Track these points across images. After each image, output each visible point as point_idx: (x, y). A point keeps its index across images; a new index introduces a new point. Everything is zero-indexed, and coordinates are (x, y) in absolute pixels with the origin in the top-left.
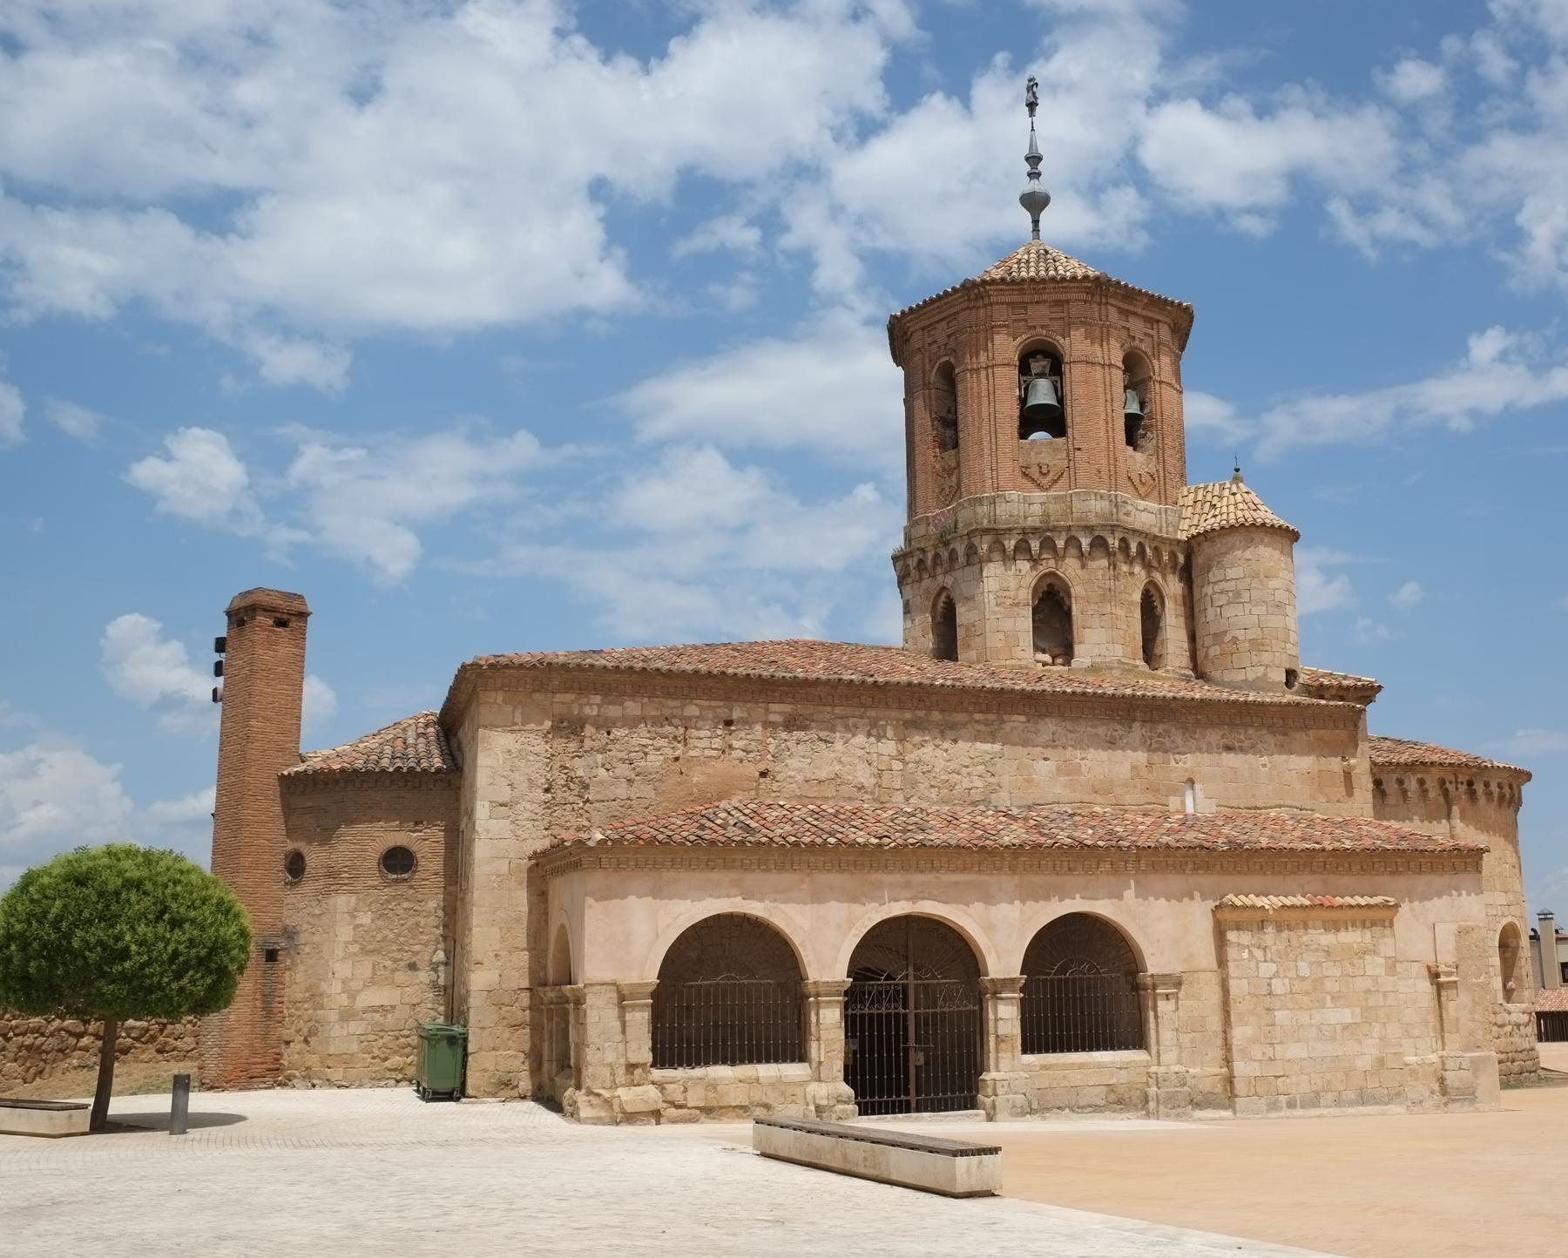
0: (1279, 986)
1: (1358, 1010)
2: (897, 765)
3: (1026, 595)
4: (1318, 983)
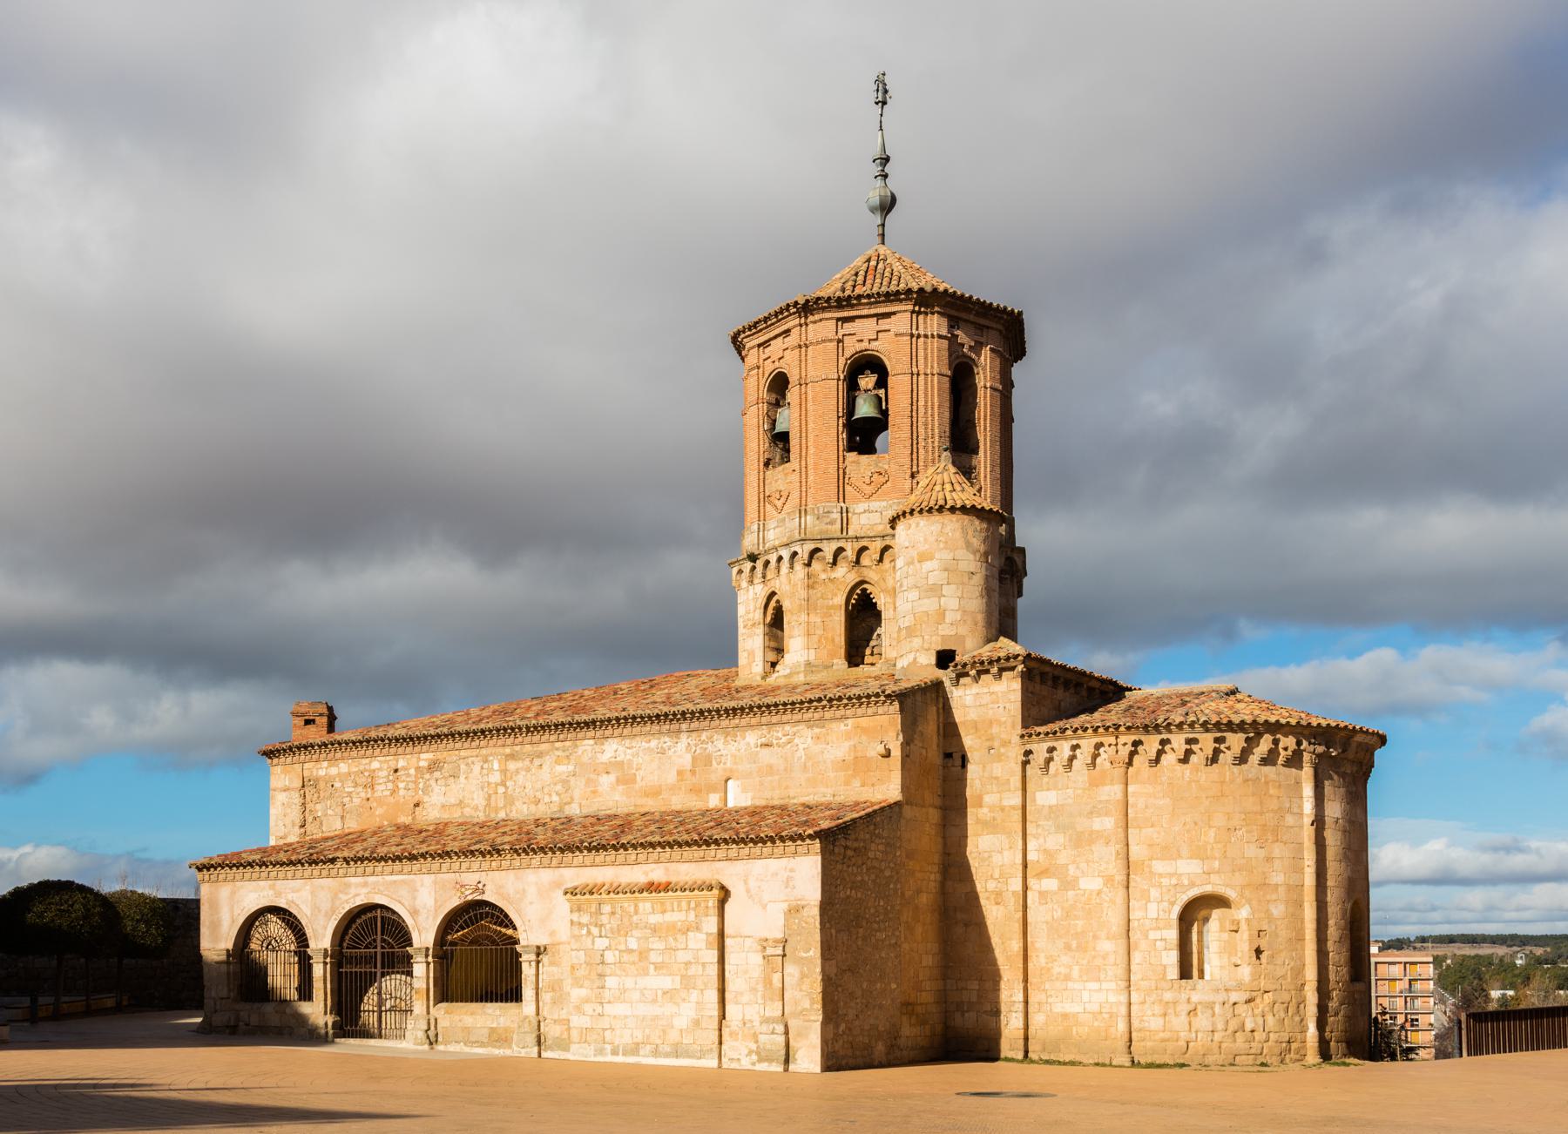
0: (610, 957)
1: (678, 979)
2: (501, 790)
3: (759, 615)
4: (643, 954)
